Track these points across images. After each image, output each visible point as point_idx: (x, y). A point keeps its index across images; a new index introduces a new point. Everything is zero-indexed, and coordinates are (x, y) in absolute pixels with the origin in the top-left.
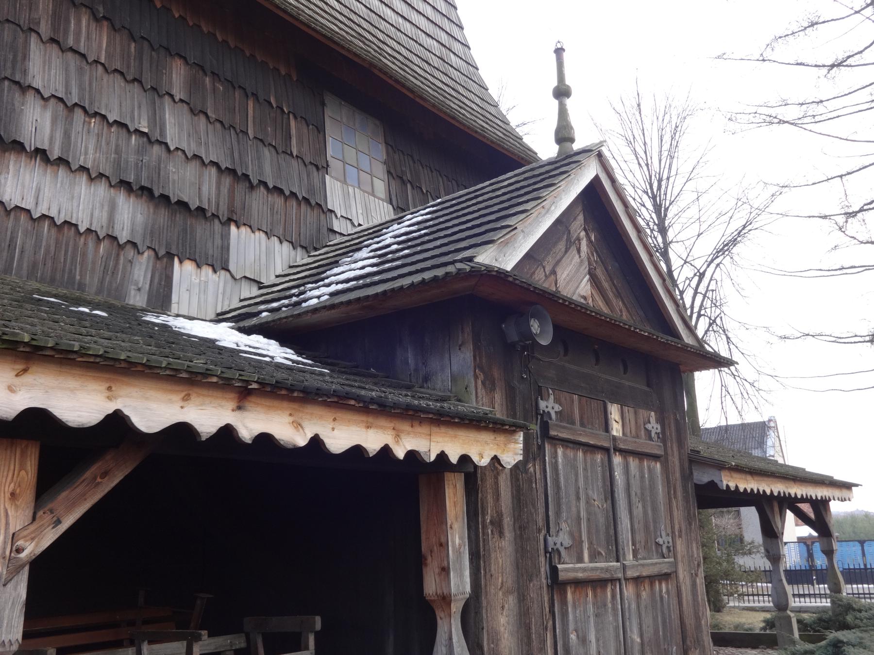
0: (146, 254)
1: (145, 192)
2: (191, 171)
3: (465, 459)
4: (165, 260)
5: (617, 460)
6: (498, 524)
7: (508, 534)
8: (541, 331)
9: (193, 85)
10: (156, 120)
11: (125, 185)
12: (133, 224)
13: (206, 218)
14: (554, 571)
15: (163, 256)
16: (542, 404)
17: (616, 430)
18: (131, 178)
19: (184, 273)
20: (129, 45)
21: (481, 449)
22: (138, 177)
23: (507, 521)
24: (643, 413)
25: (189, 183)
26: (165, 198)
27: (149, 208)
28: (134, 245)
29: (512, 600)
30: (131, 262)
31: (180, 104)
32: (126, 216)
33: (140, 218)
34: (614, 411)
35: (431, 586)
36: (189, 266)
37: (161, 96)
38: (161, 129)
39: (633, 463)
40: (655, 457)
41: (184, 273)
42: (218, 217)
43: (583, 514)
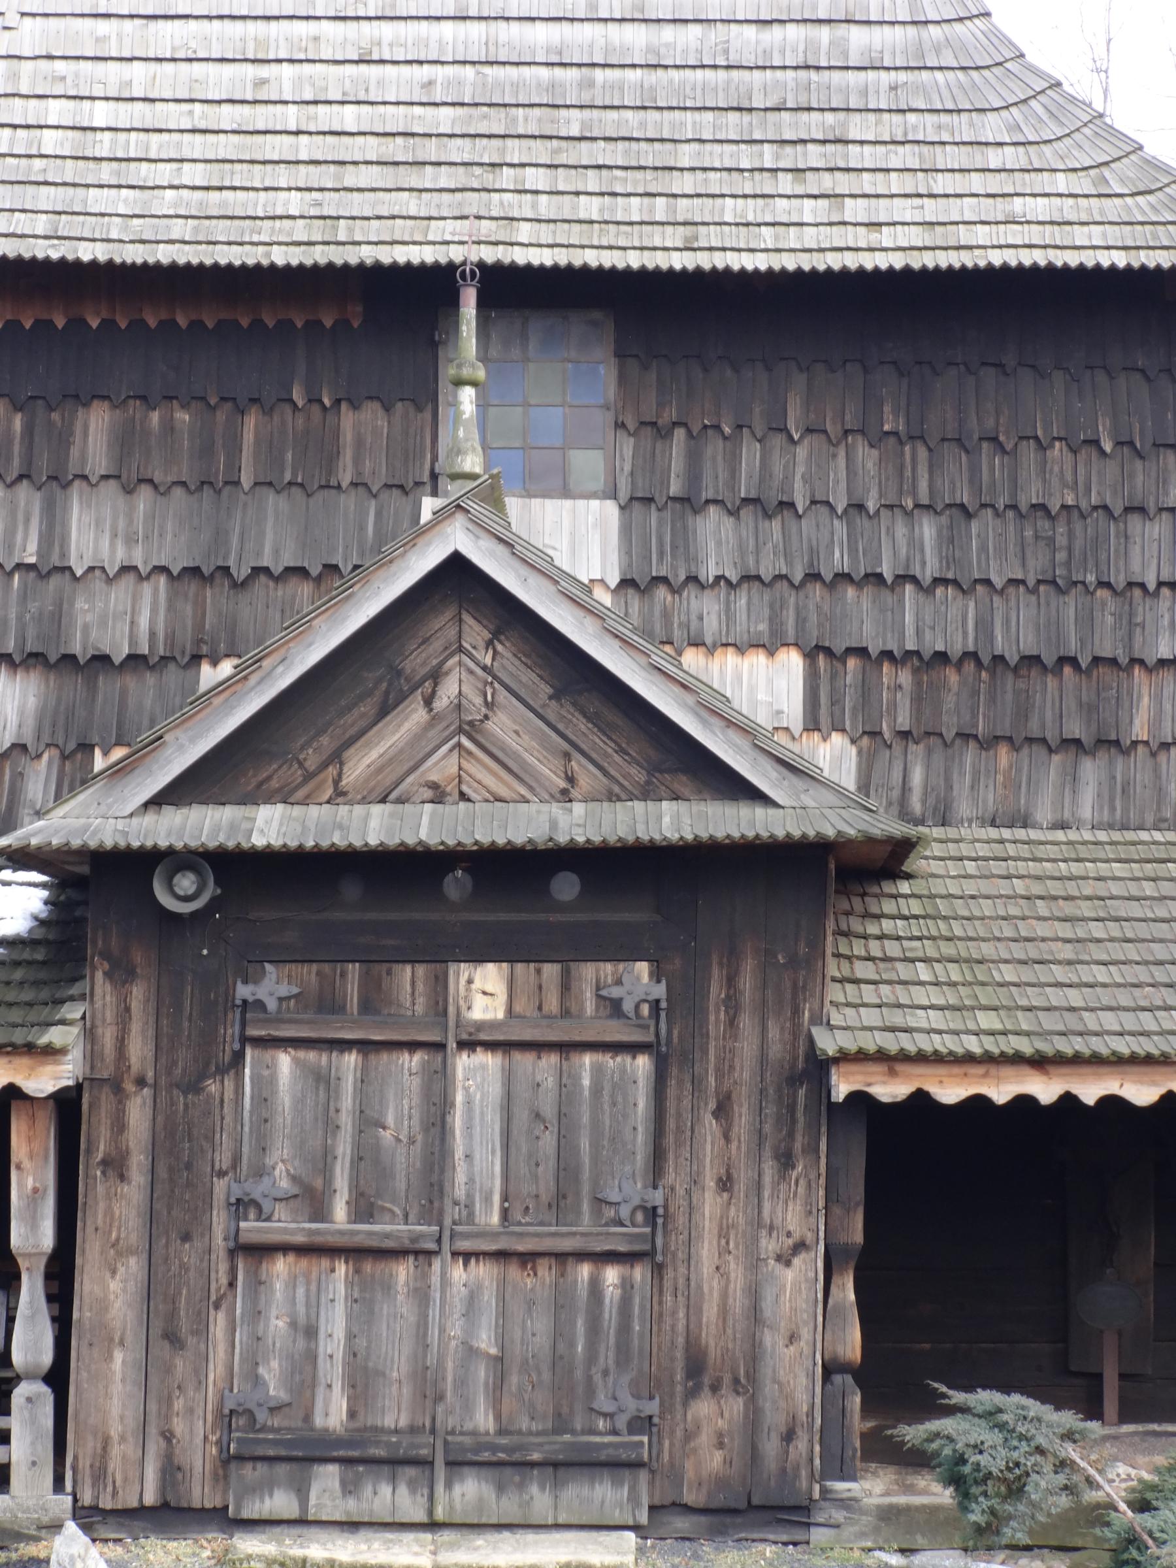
0: (46, 757)
1: (33, 660)
2: (119, 595)
4: (79, 756)
6: (116, 1166)
7: (138, 1175)
9: (125, 441)
10: (53, 532)
12: (22, 713)
13: (152, 668)
15: (74, 752)
20: (10, 421)
22: (22, 639)
23: (138, 1162)
24: (589, 973)
26: (69, 659)
27: (47, 680)
28: (23, 747)
29: (134, 1266)
30: (21, 774)
31: (102, 483)
32: (9, 707)
33: (32, 702)
37: (66, 486)
38: (62, 547)
40: (633, 1048)
42: (174, 658)
43: (344, 1148)
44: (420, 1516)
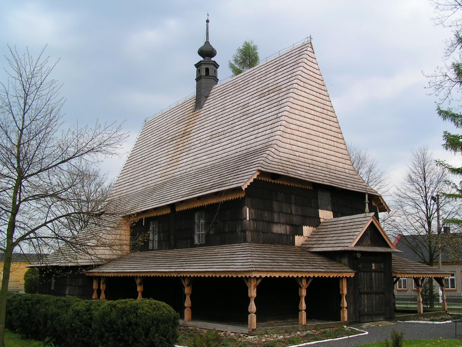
3: (346, 277)
5: (373, 274)
8: (359, 256)
10: (291, 210)
11: (288, 224)
14: (360, 291)
16: (359, 266)
17: (373, 268)
18: (288, 223)
19: (297, 237)
21: (348, 275)
25: (296, 220)
26: (293, 224)
34: (373, 265)
35: (341, 293)
36: (297, 236)
39: (377, 274)
41: (297, 237)
44: (371, 321)
